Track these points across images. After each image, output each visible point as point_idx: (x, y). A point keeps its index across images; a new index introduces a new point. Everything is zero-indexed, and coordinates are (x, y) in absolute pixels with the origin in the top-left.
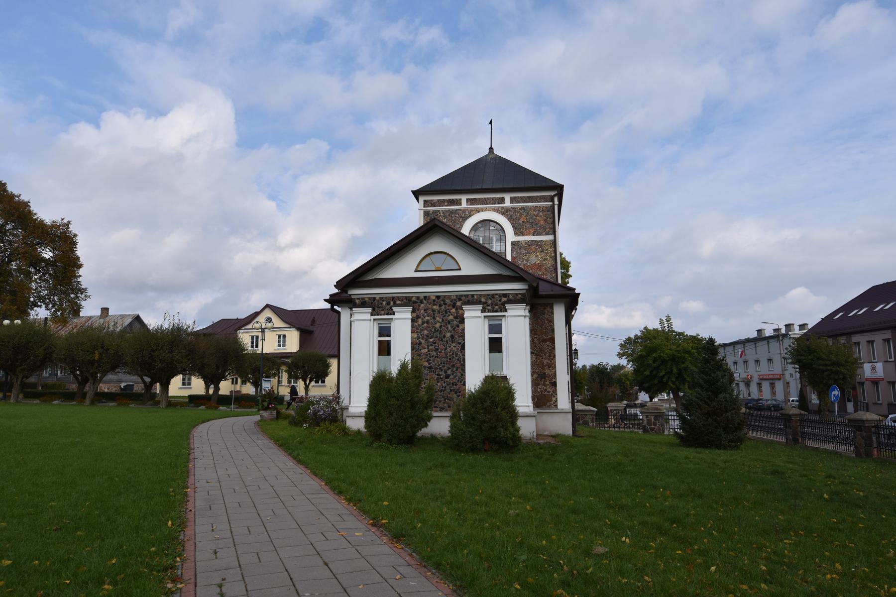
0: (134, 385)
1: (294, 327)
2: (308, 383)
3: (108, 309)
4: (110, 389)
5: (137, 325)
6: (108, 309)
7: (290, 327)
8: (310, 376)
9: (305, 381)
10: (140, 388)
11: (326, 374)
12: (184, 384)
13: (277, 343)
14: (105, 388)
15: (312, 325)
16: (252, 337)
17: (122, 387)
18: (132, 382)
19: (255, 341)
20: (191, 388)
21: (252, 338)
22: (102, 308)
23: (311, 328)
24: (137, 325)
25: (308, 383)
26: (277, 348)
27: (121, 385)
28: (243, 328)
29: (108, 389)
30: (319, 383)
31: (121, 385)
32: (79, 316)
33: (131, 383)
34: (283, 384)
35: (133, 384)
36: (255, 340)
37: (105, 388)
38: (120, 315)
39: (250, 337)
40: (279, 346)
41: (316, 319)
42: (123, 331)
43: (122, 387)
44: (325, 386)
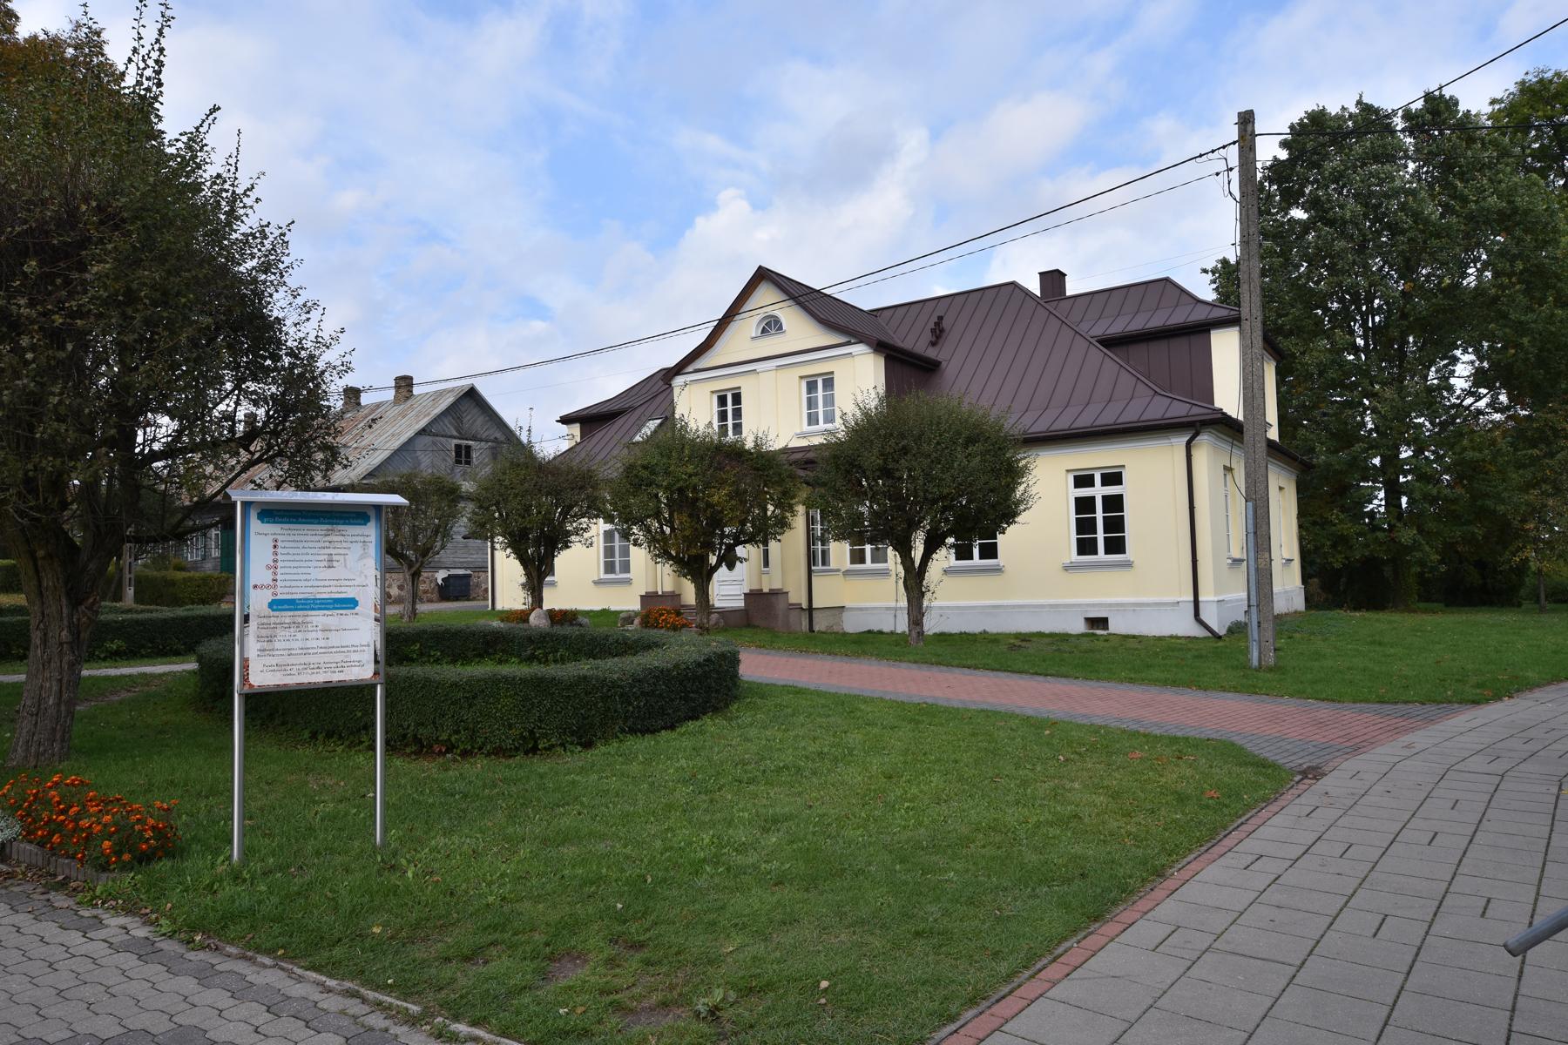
0: (470, 576)
1: (861, 339)
2: (918, 552)
7: (848, 343)
8: (926, 523)
9: (904, 549)
11: (1007, 512)
12: (609, 568)
13: (805, 411)
15: (933, 344)
16: (719, 397)
17: (440, 582)
18: (466, 568)
19: (731, 403)
21: (722, 401)
23: (931, 353)
25: (918, 552)
26: (806, 428)
27: (436, 575)
28: (690, 369)
30: (971, 558)
32: (359, 404)
34: (833, 565)
35: (469, 572)
36: (730, 408)
38: (436, 392)
39: (715, 398)
40: (812, 419)
41: (946, 324)
42: (549, 462)
43: (440, 582)
44: (998, 570)
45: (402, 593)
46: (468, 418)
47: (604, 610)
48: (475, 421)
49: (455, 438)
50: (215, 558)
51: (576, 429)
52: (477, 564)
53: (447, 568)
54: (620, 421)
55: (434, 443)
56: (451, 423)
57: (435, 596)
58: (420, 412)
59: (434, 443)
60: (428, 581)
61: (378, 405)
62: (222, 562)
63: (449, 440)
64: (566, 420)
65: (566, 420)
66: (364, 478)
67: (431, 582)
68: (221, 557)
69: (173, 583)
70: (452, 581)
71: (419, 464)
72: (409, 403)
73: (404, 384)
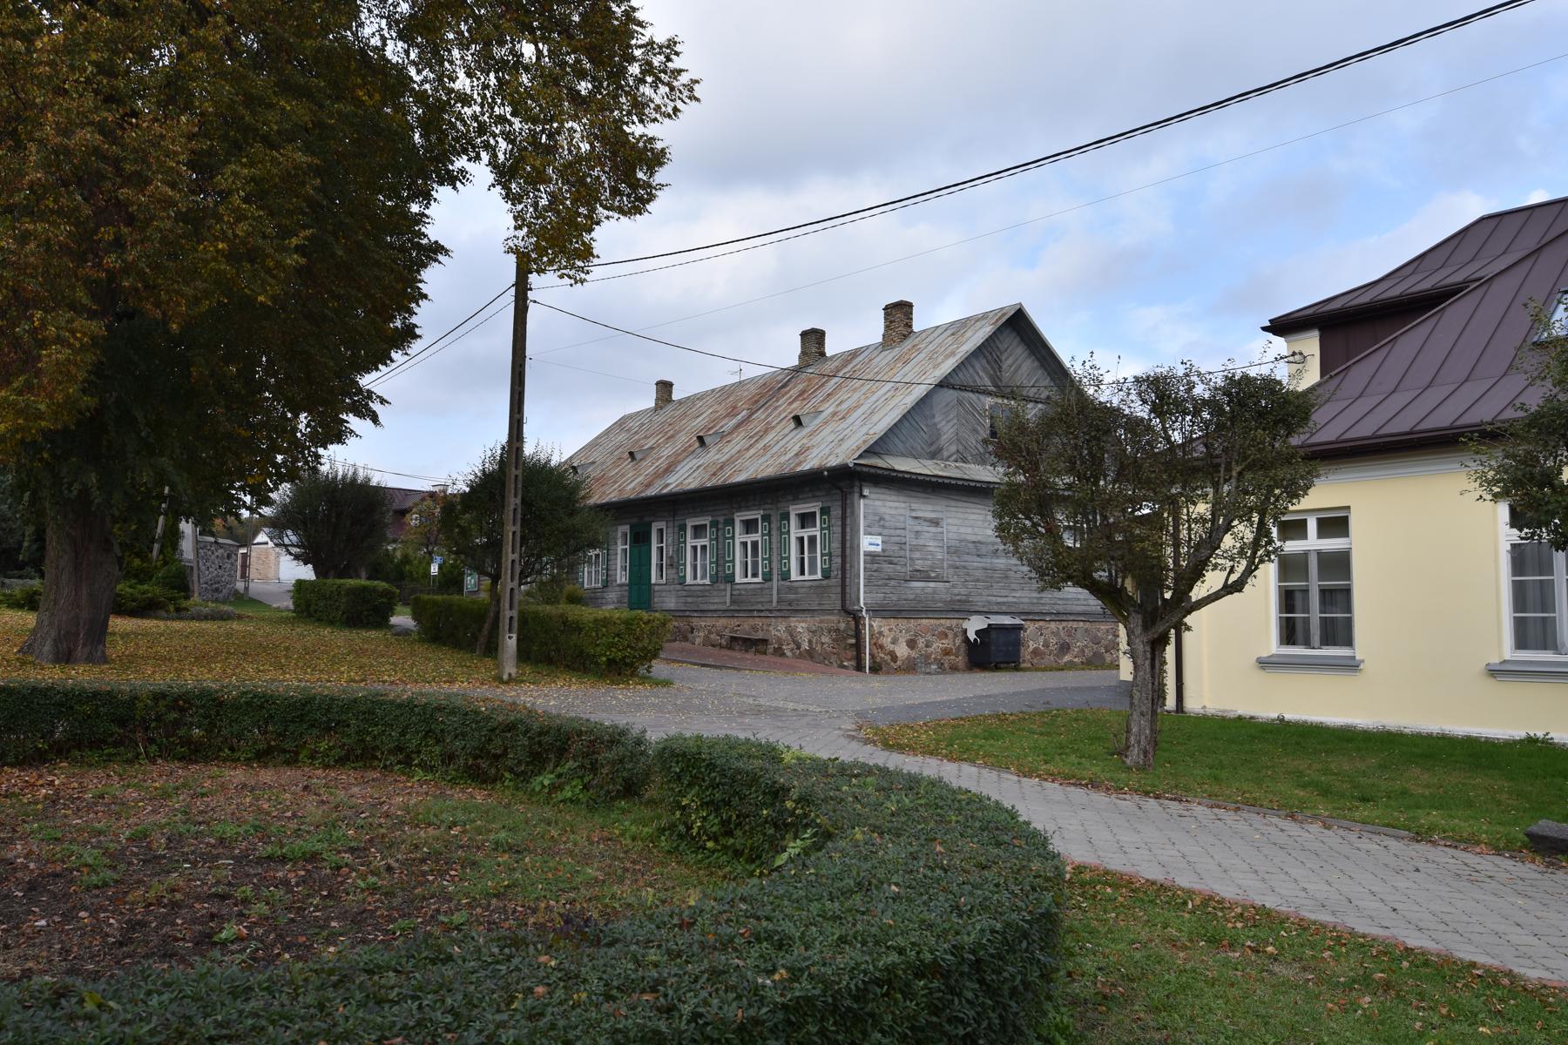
0: (1019, 628)
3: (910, 305)
4: (921, 643)
5: (1019, 366)
6: (910, 305)
10: (1053, 640)
14: (894, 641)
17: (972, 636)
20: (1352, 666)
22: (885, 309)
24: (1019, 366)
27: (966, 625)
29: (911, 644)
31: (966, 625)
32: (823, 354)
33: (1007, 620)
35: (1017, 621)
37: (894, 641)
38: (953, 324)
43: (972, 636)
45: (914, 654)
46: (1009, 362)
47: (1531, 741)
48: (1020, 367)
49: (990, 394)
50: (621, 585)
51: (1310, 344)
52: (1021, 608)
53: (986, 613)
54: (1454, 315)
55: (960, 403)
56: (984, 369)
57: (961, 660)
58: (934, 352)
59: (960, 403)
60: (951, 635)
61: (854, 354)
62: (630, 591)
63: (982, 397)
64: (1281, 327)
65: (1281, 327)
66: (860, 457)
67: (956, 635)
68: (630, 584)
69: (577, 628)
70: (994, 635)
71: (939, 436)
72: (908, 344)
73: (899, 314)
